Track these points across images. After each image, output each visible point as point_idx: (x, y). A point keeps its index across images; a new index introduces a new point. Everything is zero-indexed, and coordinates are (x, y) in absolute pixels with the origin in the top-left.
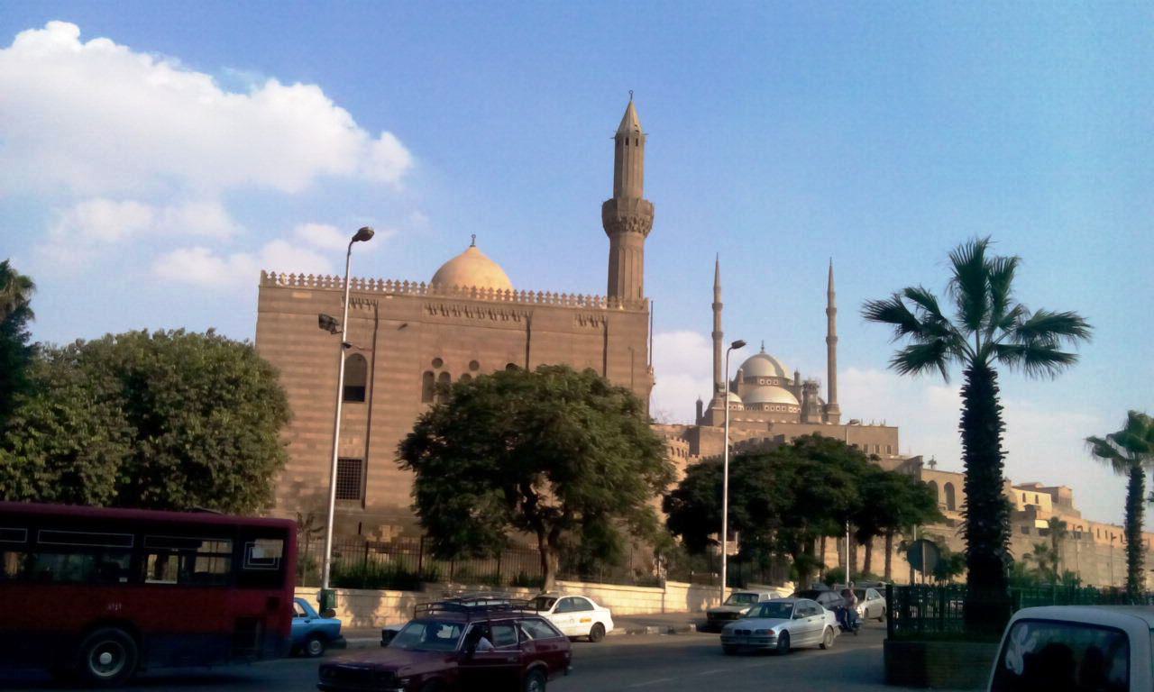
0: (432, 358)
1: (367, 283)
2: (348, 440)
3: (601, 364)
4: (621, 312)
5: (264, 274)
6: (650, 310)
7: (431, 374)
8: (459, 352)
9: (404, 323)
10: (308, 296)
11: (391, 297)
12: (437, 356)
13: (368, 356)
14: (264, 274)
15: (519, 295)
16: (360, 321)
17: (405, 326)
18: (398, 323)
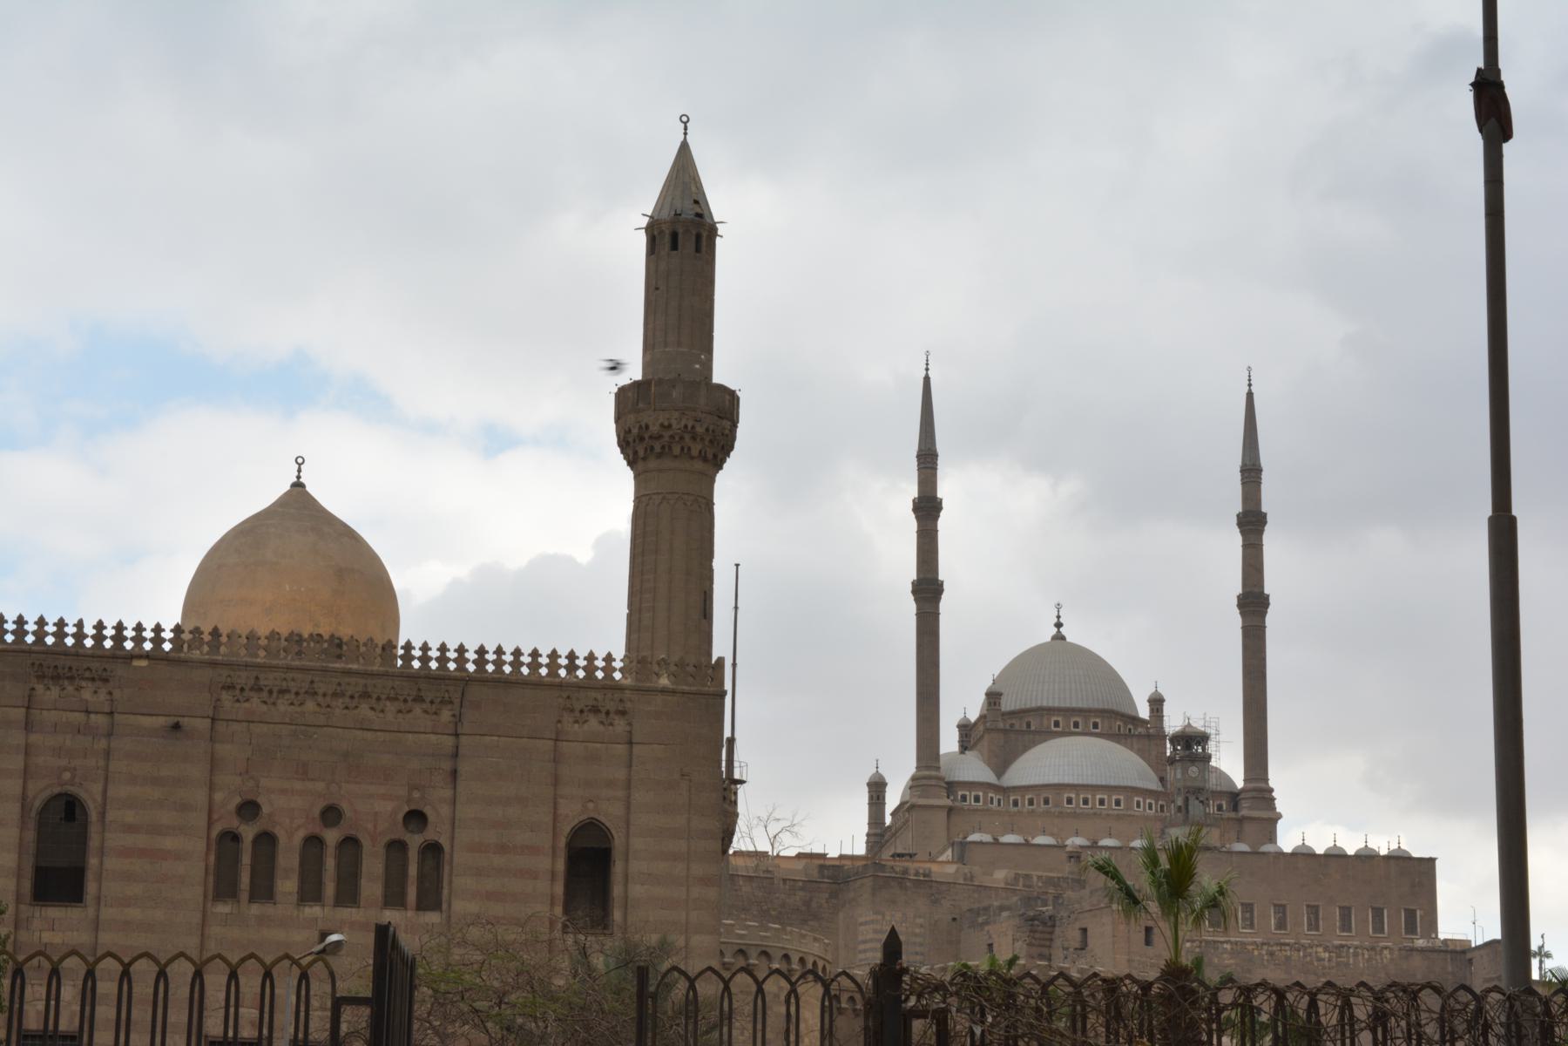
0: (238, 800)
1: (89, 630)
4: (664, 691)
6: (728, 686)
7: (235, 838)
8: (298, 785)
9: (176, 719)
11: (144, 663)
12: (249, 797)
13: (90, 795)
15: (434, 653)
16: (79, 717)
17: (177, 727)
18: (161, 721)
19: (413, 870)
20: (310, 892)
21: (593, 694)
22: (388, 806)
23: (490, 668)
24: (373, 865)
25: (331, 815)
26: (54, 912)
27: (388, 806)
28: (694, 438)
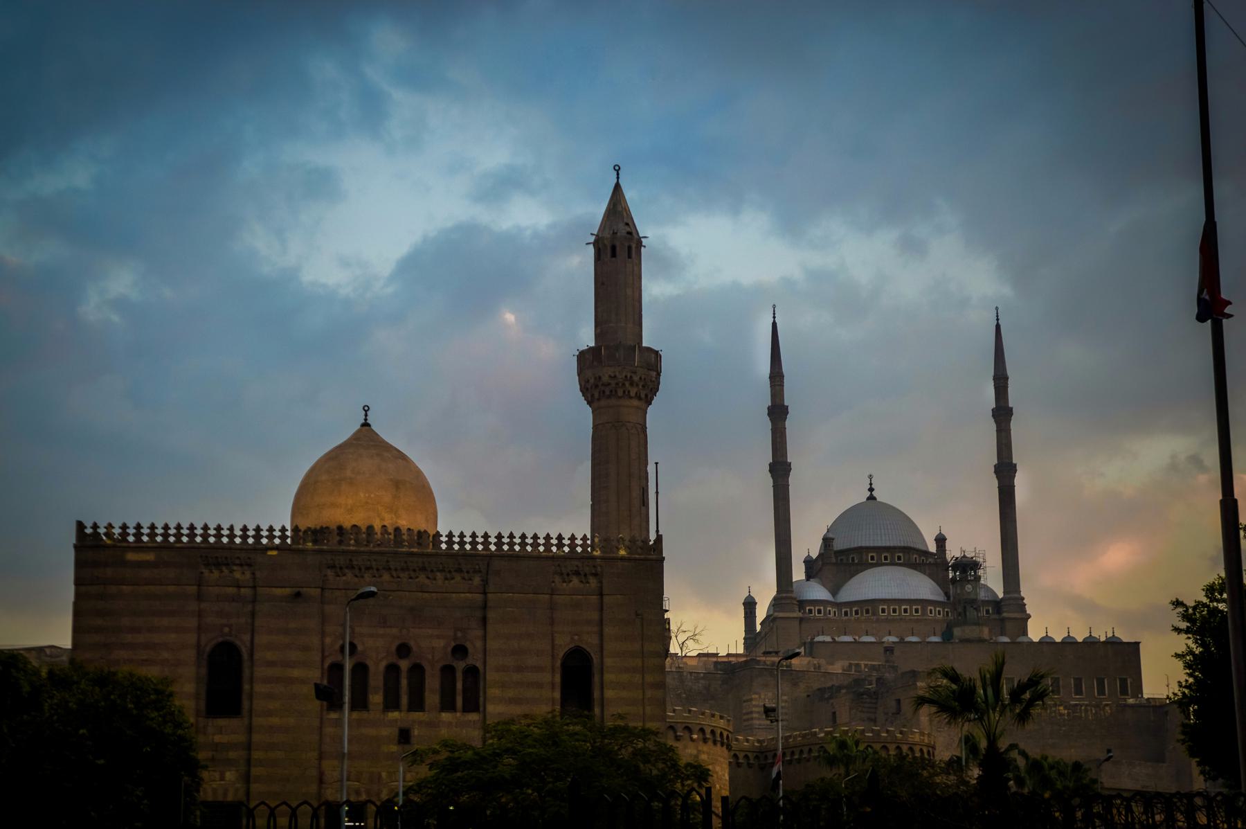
2: (217, 775)
3: (595, 640)
4: (622, 559)
5: (80, 526)
8: (381, 631)
9: (297, 590)
10: (150, 557)
11: (275, 553)
13: (243, 641)
14: (80, 526)
16: (231, 590)
17: (298, 595)
18: (288, 591)
19: (459, 685)
20: (392, 703)
21: (576, 563)
22: (442, 643)
23: (506, 547)
24: (432, 683)
25: (403, 650)
26: (222, 722)
27: (442, 643)
28: (631, 384)
